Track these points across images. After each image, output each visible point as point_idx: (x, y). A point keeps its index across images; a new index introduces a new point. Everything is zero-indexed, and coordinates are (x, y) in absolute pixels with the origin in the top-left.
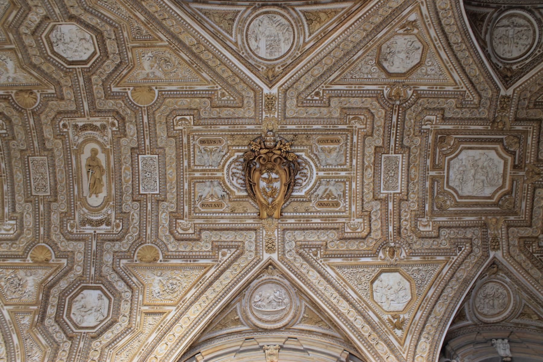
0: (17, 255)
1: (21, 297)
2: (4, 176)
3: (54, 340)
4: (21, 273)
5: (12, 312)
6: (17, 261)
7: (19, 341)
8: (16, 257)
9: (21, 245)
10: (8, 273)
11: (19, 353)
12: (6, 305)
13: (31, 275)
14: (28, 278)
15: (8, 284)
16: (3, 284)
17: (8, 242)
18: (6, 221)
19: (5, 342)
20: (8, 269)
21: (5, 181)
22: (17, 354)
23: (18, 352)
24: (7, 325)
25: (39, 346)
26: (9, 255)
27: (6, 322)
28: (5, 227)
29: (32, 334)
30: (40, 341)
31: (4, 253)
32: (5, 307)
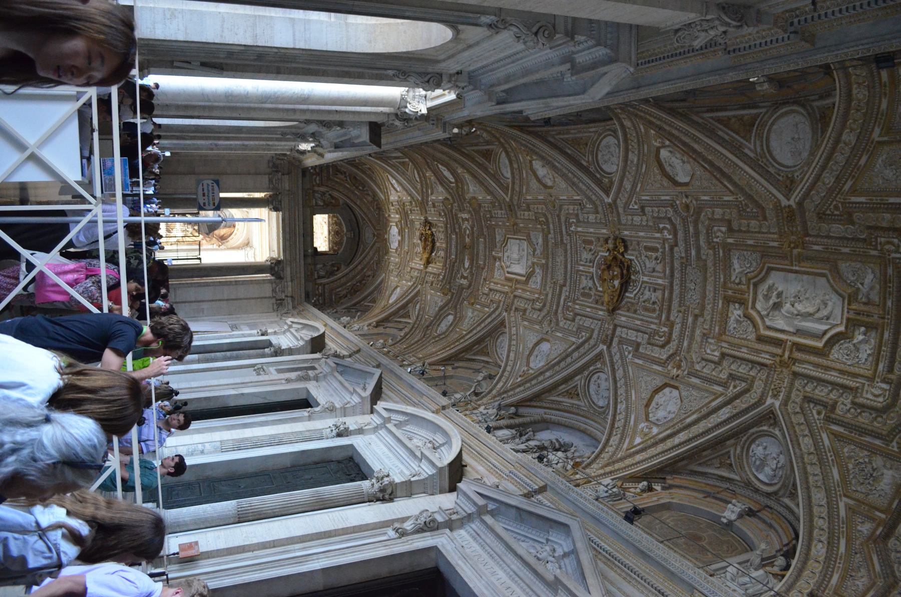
0: (878, 434)
1: (869, 494)
2: (888, 319)
3: (893, 572)
4: (878, 461)
5: (850, 508)
6: (878, 442)
7: (846, 551)
8: (878, 436)
9: (888, 422)
10: (861, 455)
11: (841, 565)
12: (845, 496)
13: (891, 469)
14: (885, 471)
15: (857, 470)
16: (850, 466)
17: (872, 412)
18: (877, 382)
19: (829, 543)
20: (863, 449)
21: (887, 326)
22: (837, 565)
23: (840, 563)
24: (838, 522)
25: (869, 571)
26: (868, 430)
27: (838, 519)
28: (872, 390)
29: (865, 548)
30: (873, 565)
31: (863, 426)
32: (844, 499)
